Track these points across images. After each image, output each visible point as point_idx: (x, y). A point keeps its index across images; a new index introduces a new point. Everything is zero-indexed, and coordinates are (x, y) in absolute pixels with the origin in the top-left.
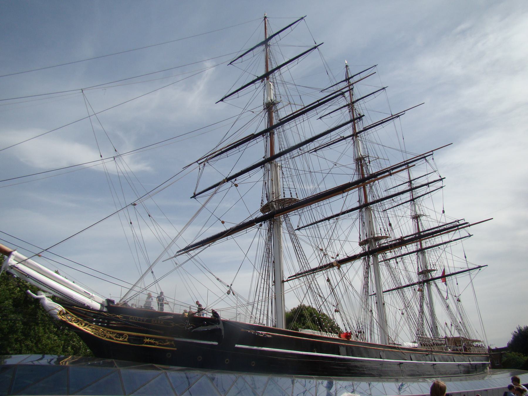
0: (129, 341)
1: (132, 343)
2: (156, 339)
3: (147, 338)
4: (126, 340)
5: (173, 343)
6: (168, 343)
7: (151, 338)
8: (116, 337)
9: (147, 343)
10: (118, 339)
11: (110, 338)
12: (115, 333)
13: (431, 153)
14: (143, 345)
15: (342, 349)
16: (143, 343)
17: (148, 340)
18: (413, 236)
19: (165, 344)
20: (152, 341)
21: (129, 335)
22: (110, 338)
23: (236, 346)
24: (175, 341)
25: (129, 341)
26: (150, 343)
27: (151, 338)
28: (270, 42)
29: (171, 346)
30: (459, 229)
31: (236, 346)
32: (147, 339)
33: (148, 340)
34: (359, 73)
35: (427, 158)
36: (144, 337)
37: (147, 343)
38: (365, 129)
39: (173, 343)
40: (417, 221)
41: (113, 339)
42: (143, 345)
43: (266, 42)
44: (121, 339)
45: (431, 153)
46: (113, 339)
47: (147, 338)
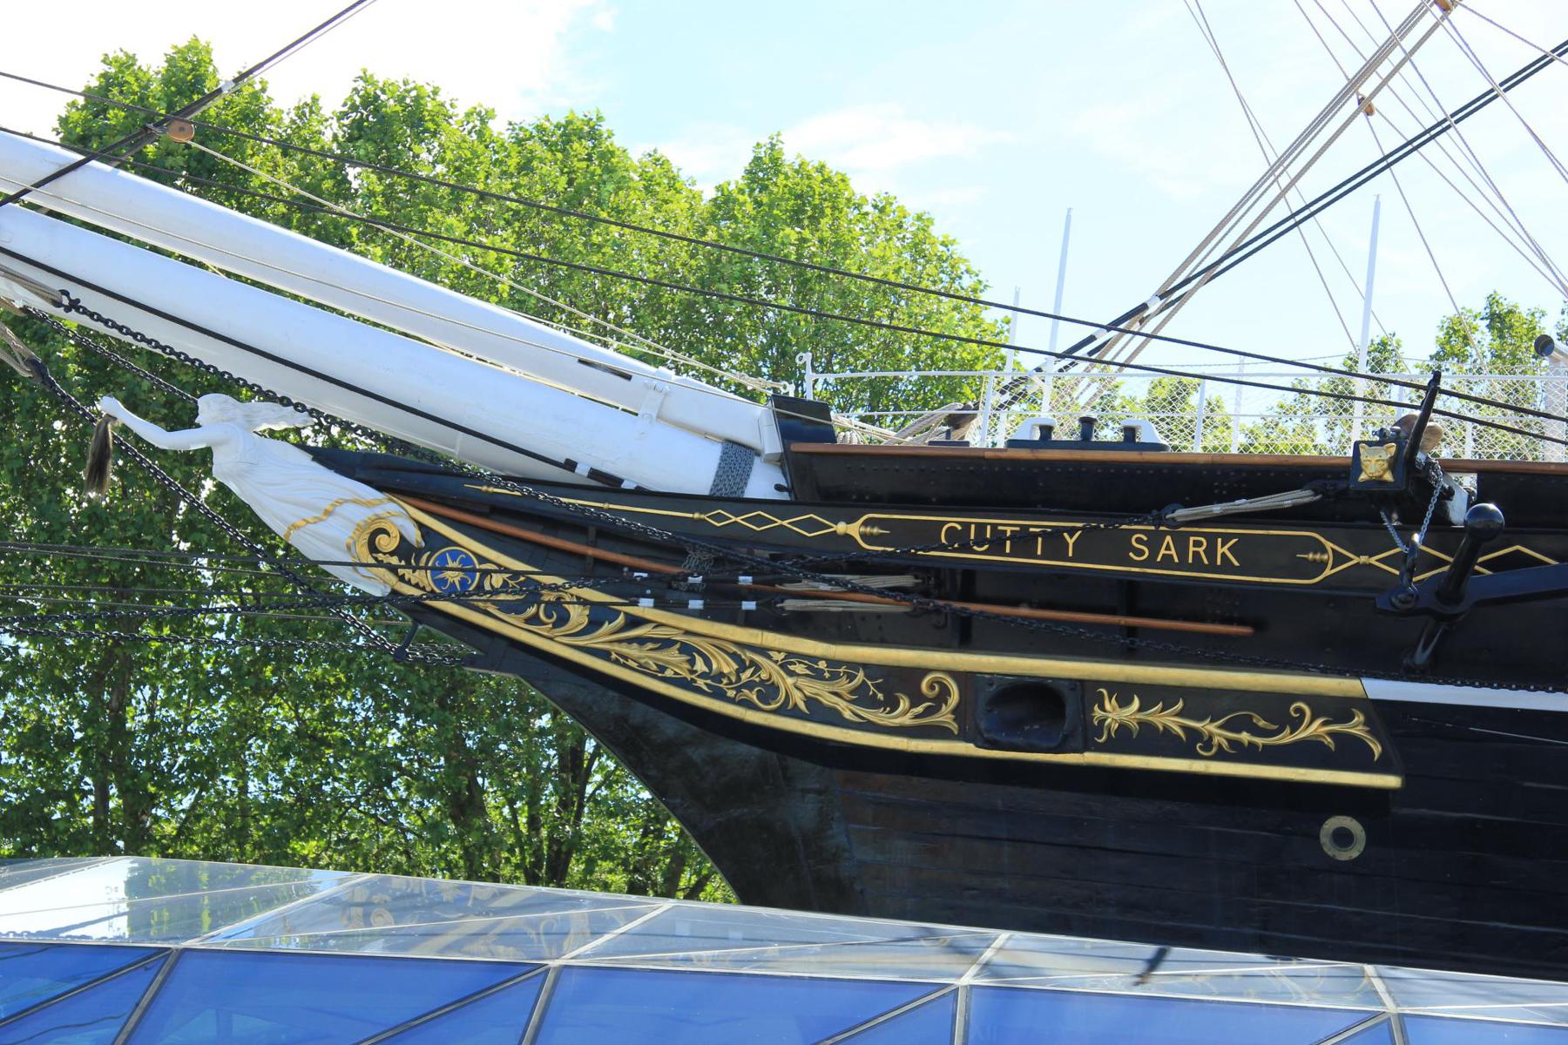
2: (1200, 701)
3: (1124, 692)
4: (945, 717)
5: (1356, 727)
6: (1314, 729)
8: (861, 697)
9: (1124, 740)
10: (878, 716)
11: (817, 711)
12: (854, 666)
17: (1130, 713)
19: (1286, 738)
20: (1168, 719)
22: (817, 711)
27: (1152, 694)
29: (1349, 754)
32: (1124, 702)
33: (1130, 713)
36: (1087, 690)
37: (1124, 740)
39: (1356, 727)
41: (832, 717)
44: (905, 714)
46: (832, 717)
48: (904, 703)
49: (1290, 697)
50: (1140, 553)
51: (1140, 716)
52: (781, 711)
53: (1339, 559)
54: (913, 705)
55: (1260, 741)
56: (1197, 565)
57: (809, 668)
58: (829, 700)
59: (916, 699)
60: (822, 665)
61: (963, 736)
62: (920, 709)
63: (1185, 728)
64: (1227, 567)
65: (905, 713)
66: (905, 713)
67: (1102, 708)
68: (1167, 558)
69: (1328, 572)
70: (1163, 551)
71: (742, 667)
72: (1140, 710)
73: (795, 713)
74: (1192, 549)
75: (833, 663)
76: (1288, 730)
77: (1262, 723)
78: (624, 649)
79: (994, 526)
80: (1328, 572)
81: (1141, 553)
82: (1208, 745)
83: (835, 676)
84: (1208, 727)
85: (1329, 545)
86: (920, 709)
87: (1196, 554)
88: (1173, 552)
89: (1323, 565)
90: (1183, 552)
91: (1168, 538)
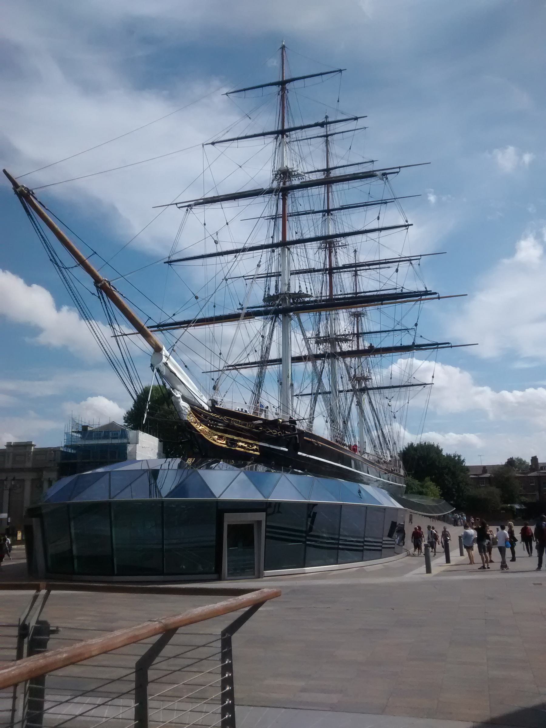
6: (255, 447)
7: (243, 442)
9: (239, 447)
13: (419, 257)
15: (353, 462)
18: (263, 309)
22: (214, 440)
23: (299, 453)
24: (260, 446)
25: (226, 444)
26: (242, 447)
28: (288, 86)
30: (437, 348)
31: (299, 453)
33: (240, 444)
34: (343, 132)
35: (412, 262)
38: (342, 208)
40: (358, 319)
43: (283, 84)
45: (419, 257)
47: (240, 441)
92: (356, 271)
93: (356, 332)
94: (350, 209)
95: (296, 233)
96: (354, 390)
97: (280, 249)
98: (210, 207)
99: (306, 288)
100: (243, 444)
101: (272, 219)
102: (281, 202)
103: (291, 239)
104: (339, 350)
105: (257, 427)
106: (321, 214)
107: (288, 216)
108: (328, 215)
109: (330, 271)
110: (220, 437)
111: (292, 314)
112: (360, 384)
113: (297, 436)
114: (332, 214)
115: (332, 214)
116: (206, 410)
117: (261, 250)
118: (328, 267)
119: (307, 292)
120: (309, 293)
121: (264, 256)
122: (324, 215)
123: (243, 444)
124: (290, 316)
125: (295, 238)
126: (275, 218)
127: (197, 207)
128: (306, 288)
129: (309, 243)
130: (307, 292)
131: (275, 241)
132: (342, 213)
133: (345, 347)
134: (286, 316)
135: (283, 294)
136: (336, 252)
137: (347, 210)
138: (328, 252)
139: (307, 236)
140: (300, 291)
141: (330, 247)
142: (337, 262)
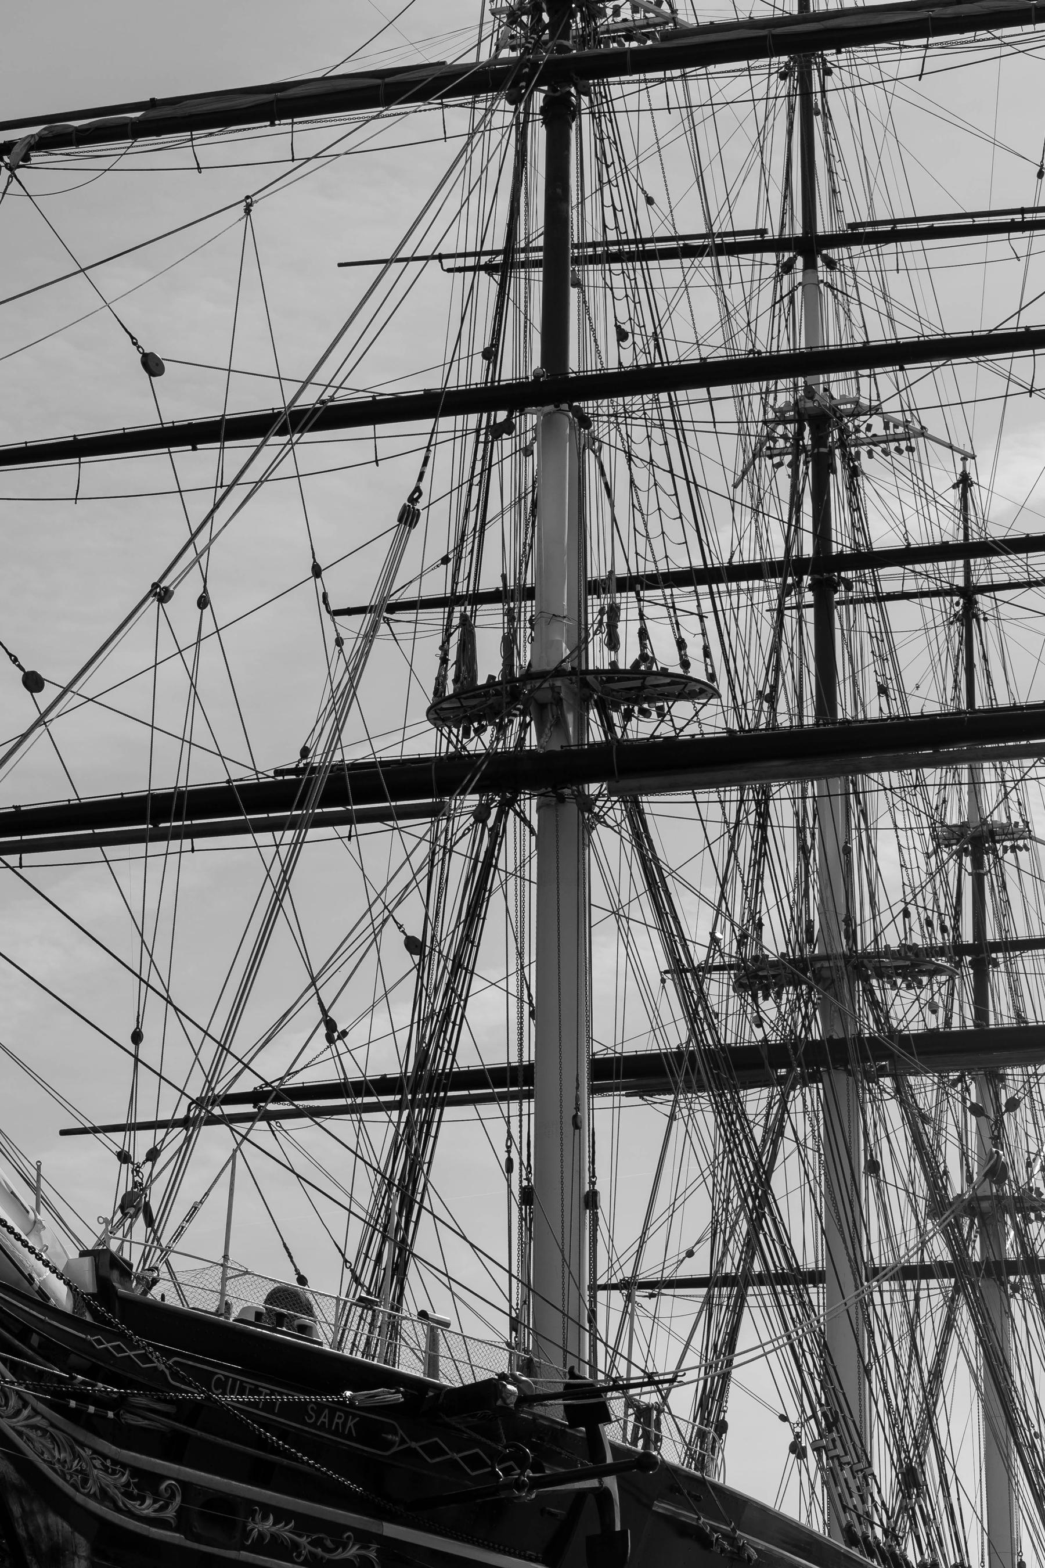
0: (182, 1524)
1: (198, 1539)
2: (305, 1523)
3: (267, 1509)
4: (170, 1513)
7: (282, 1515)
10: (134, 1505)
12: (124, 1466)
14: (245, 1556)
16: (238, 1537)
17: (268, 1526)
21: (186, 1486)
22: (103, 1496)
27: (282, 1515)
32: (265, 1518)
33: (268, 1526)
36: (250, 1507)
40: (978, 864)
42: (245, 1556)
44: (148, 1508)
48: (148, 1502)
49: (347, 1528)
50: (310, 1417)
51: (273, 1529)
52: (88, 1495)
53: (403, 1441)
54: (155, 1502)
55: (327, 1556)
56: (336, 1433)
57: (102, 1464)
58: (112, 1491)
59: (157, 1496)
60: (108, 1463)
61: (176, 1530)
62: (157, 1506)
63: (292, 1540)
64: (349, 1437)
65: (148, 1508)
66: (148, 1508)
67: (253, 1520)
68: (323, 1423)
69: (395, 1449)
70: (322, 1419)
71: (76, 1455)
72: (274, 1524)
73: (93, 1497)
74: (336, 1420)
75: (115, 1462)
76: (340, 1550)
77: (329, 1543)
78: (32, 1434)
79: (242, 1382)
80: (395, 1449)
81: (310, 1417)
82: (299, 1555)
83: (114, 1472)
84: (303, 1541)
85: (400, 1432)
86: (157, 1506)
87: (337, 1423)
88: (326, 1421)
89: (392, 1444)
90: (331, 1421)
91: (326, 1411)
92: (969, 593)
93: (968, 936)
94: (928, 243)
95: (622, 335)
96: (957, 1269)
97: (532, 419)
98: (126, 162)
99: (681, 644)
100: (285, 1531)
101: (490, 269)
102: (539, 135)
103: (592, 366)
104: (869, 1026)
105: (370, 1425)
106: (770, 257)
107: (576, 261)
108: (810, 265)
109: (825, 574)
110: (147, 1482)
111: (593, 788)
112: (992, 1237)
113: (611, 1483)
114: (831, 264)
115: (831, 264)
116: (57, 1313)
117: (427, 424)
118: (808, 550)
119: (685, 664)
120: (698, 671)
121: (443, 455)
122: (787, 268)
123: (285, 1531)
124: (586, 804)
125: (616, 357)
126: (504, 265)
127: (57, 157)
128: (681, 644)
129: (701, 393)
130: (685, 664)
131: (507, 373)
132: (889, 262)
133: (909, 1009)
134: (561, 799)
135: (543, 675)
136: (854, 472)
137: (916, 244)
138: (807, 470)
139: (679, 351)
140: (644, 657)
141: (819, 439)
142: (859, 526)
